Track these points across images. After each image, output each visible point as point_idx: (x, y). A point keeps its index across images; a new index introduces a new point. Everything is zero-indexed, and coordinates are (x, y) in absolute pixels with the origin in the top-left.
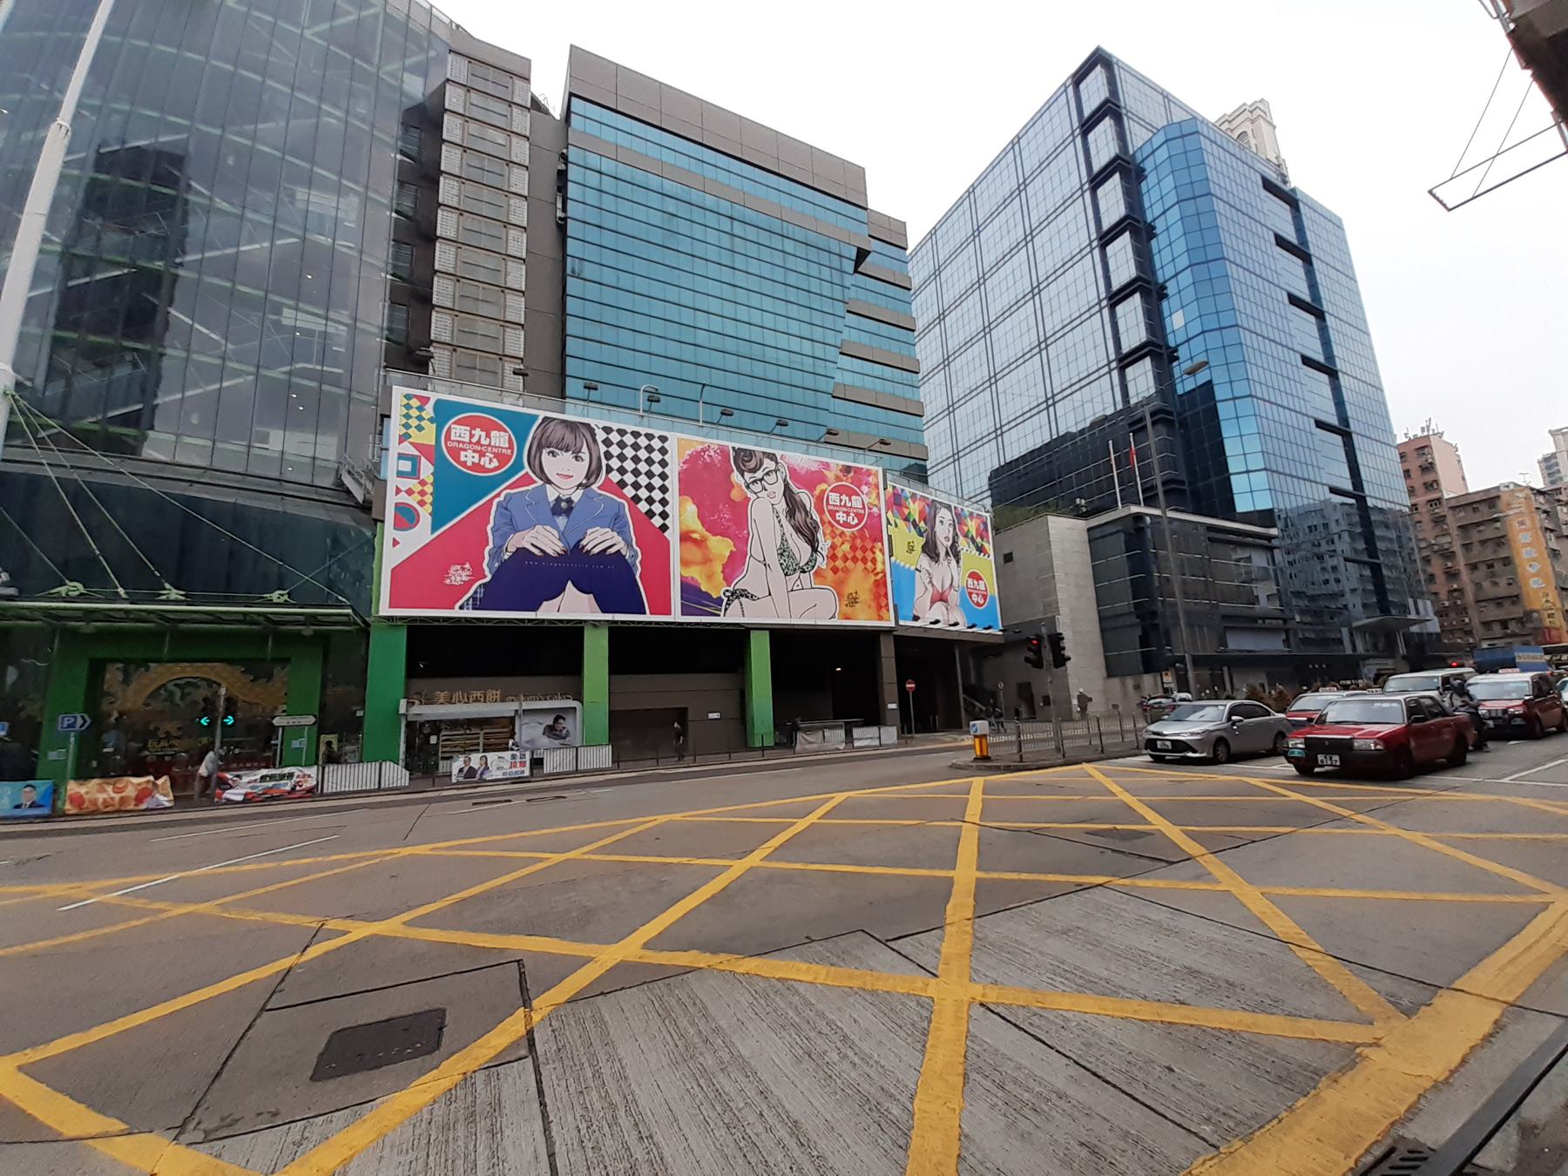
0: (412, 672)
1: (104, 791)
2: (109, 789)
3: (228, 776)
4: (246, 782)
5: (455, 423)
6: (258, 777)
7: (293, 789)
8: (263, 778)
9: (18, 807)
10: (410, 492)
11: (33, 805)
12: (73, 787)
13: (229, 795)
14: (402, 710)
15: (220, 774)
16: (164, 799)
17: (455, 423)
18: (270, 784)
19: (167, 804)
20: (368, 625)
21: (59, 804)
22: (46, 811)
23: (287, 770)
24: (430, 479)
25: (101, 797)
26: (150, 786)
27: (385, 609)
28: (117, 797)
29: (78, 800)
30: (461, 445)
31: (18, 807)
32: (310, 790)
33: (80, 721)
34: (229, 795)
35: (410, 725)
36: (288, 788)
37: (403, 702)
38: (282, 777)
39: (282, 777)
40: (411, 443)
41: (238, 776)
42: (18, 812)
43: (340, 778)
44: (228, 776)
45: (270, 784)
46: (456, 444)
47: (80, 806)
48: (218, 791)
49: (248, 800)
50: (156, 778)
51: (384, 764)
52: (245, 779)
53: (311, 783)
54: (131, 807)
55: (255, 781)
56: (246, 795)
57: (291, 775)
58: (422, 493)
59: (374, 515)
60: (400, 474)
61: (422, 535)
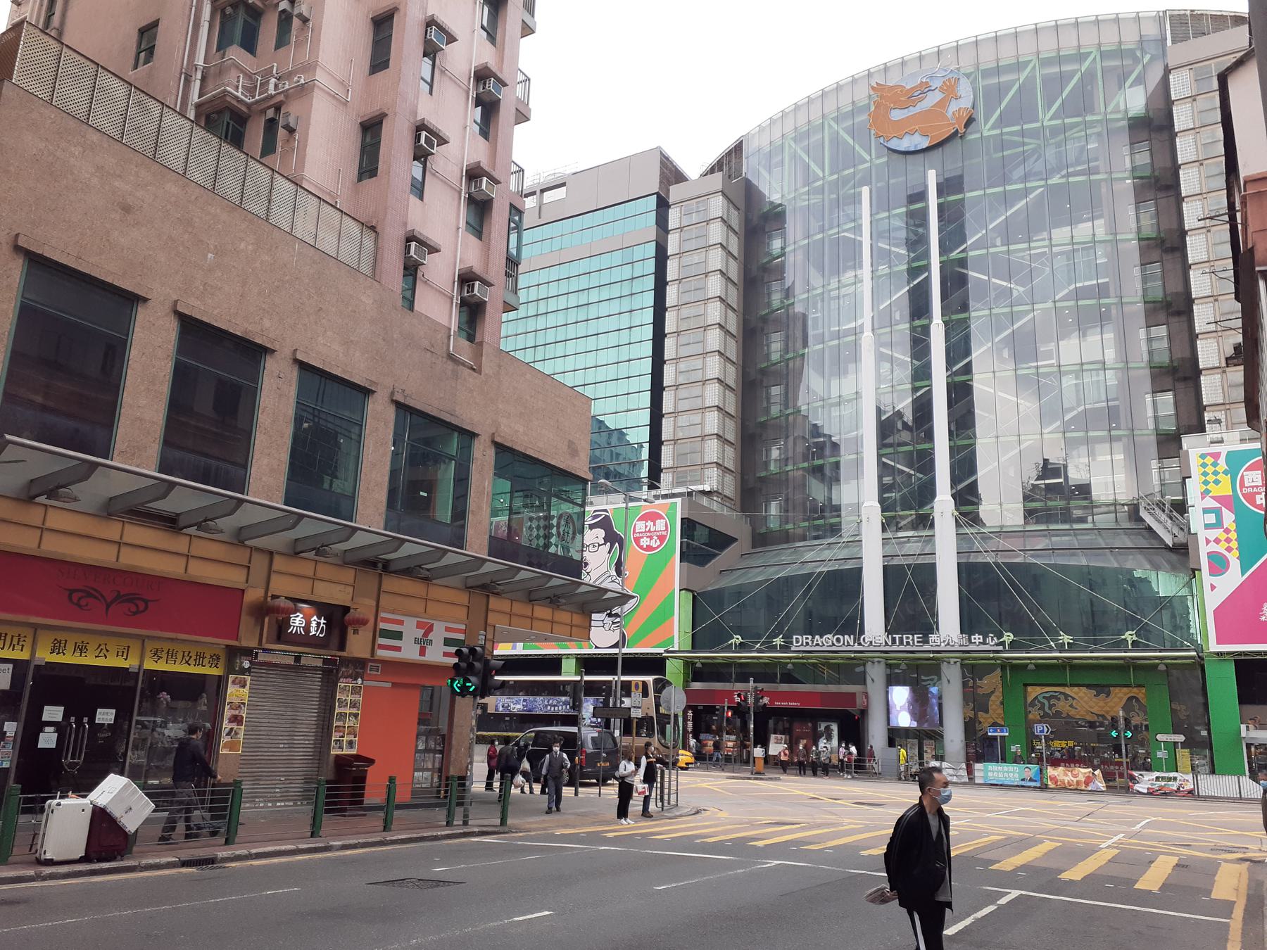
0: (1243, 699)
1: (1067, 775)
2: (1069, 774)
3: (1136, 774)
4: (1146, 781)
5: (1246, 470)
6: (1154, 777)
7: (1178, 789)
8: (1157, 778)
9: (1023, 780)
10: (1217, 541)
11: (1031, 780)
12: (1051, 771)
13: (1137, 787)
14: (1243, 734)
15: (1129, 772)
16: (1101, 785)
17: (1246, 470)
18: (1163, 783)
19: (1104, 789)
20: (1203, 659)
21: (1045, 780)
22: (1038, 784)
23: (1172, 774)
24: (1233, 527)
25: (1066, 779)
26: (1091, 775)
27: (1214, 647)
28: (1075, 780)
29: (1054, 779)
30: (1255, 490)
31: (1023, 780)
32: (1191, 792)
33: (1046, 730)
34: (1137, 787)
35: (1249, 746)
36: (1175, 788)
37: (1243, 727)
38: (1170, 779)
39: (1170, 779)
40: (1211, 497)
41: (1141, 775)
42: (1023, 783)
43: (1211, 784)
44: (1136, 774)
45: (1163, 783)
46: (1250, 490)
47: (1056, 782)
48: (1131, 784)
49: (1151, 793)
50: (1094, 770)
51: (1241, 778)
52: (1146, 778)
53: (1190, 786)
54: (1083, 788)
55: (1153, 780)
56: (1148, 789)
57: (1175, 779)
58: (1228, 540)
59: (1192, 566)
60: (1208, 526)
61: (1233, 578)
